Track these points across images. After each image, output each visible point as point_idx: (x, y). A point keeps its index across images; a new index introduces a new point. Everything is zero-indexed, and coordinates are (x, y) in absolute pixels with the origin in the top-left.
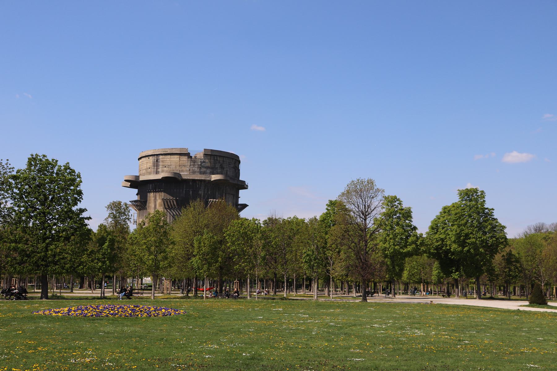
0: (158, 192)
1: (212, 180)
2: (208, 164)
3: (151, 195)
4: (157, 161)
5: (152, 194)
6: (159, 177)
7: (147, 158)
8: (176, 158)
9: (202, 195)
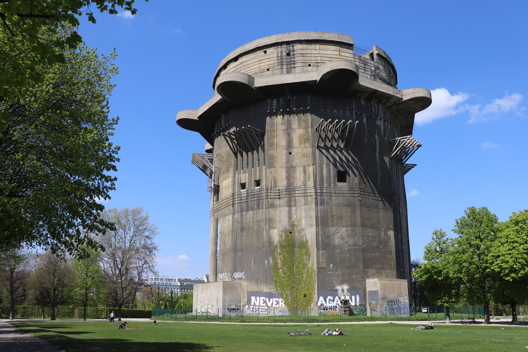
0: (297, 113)
1: (405, 99)
2: (384, 75)
3: (277, 123)
4: (288, 54)
5: (279, 119)
6: (314, 75)
7: (261, 53)
8: (331, 50)
9: (382, 128)
